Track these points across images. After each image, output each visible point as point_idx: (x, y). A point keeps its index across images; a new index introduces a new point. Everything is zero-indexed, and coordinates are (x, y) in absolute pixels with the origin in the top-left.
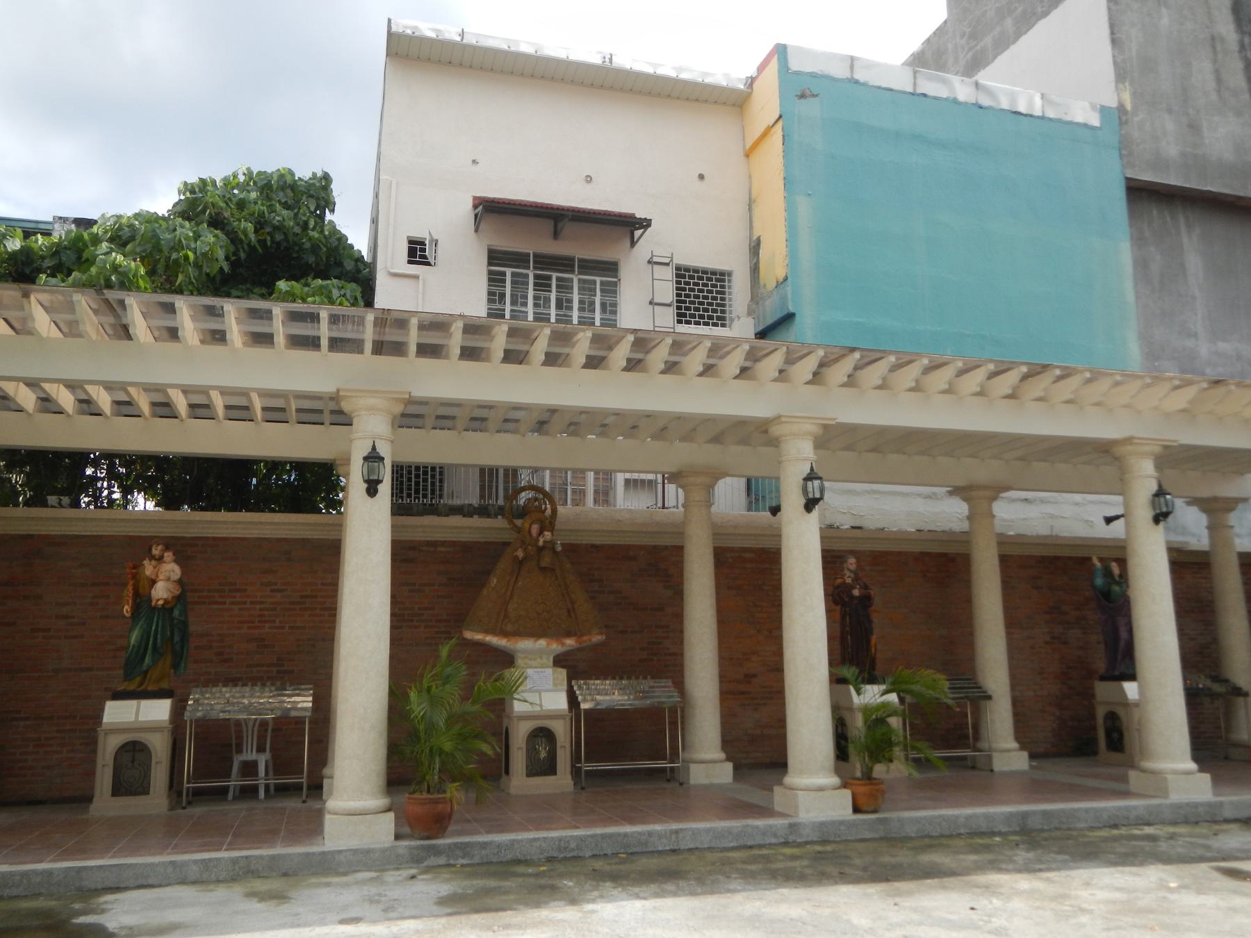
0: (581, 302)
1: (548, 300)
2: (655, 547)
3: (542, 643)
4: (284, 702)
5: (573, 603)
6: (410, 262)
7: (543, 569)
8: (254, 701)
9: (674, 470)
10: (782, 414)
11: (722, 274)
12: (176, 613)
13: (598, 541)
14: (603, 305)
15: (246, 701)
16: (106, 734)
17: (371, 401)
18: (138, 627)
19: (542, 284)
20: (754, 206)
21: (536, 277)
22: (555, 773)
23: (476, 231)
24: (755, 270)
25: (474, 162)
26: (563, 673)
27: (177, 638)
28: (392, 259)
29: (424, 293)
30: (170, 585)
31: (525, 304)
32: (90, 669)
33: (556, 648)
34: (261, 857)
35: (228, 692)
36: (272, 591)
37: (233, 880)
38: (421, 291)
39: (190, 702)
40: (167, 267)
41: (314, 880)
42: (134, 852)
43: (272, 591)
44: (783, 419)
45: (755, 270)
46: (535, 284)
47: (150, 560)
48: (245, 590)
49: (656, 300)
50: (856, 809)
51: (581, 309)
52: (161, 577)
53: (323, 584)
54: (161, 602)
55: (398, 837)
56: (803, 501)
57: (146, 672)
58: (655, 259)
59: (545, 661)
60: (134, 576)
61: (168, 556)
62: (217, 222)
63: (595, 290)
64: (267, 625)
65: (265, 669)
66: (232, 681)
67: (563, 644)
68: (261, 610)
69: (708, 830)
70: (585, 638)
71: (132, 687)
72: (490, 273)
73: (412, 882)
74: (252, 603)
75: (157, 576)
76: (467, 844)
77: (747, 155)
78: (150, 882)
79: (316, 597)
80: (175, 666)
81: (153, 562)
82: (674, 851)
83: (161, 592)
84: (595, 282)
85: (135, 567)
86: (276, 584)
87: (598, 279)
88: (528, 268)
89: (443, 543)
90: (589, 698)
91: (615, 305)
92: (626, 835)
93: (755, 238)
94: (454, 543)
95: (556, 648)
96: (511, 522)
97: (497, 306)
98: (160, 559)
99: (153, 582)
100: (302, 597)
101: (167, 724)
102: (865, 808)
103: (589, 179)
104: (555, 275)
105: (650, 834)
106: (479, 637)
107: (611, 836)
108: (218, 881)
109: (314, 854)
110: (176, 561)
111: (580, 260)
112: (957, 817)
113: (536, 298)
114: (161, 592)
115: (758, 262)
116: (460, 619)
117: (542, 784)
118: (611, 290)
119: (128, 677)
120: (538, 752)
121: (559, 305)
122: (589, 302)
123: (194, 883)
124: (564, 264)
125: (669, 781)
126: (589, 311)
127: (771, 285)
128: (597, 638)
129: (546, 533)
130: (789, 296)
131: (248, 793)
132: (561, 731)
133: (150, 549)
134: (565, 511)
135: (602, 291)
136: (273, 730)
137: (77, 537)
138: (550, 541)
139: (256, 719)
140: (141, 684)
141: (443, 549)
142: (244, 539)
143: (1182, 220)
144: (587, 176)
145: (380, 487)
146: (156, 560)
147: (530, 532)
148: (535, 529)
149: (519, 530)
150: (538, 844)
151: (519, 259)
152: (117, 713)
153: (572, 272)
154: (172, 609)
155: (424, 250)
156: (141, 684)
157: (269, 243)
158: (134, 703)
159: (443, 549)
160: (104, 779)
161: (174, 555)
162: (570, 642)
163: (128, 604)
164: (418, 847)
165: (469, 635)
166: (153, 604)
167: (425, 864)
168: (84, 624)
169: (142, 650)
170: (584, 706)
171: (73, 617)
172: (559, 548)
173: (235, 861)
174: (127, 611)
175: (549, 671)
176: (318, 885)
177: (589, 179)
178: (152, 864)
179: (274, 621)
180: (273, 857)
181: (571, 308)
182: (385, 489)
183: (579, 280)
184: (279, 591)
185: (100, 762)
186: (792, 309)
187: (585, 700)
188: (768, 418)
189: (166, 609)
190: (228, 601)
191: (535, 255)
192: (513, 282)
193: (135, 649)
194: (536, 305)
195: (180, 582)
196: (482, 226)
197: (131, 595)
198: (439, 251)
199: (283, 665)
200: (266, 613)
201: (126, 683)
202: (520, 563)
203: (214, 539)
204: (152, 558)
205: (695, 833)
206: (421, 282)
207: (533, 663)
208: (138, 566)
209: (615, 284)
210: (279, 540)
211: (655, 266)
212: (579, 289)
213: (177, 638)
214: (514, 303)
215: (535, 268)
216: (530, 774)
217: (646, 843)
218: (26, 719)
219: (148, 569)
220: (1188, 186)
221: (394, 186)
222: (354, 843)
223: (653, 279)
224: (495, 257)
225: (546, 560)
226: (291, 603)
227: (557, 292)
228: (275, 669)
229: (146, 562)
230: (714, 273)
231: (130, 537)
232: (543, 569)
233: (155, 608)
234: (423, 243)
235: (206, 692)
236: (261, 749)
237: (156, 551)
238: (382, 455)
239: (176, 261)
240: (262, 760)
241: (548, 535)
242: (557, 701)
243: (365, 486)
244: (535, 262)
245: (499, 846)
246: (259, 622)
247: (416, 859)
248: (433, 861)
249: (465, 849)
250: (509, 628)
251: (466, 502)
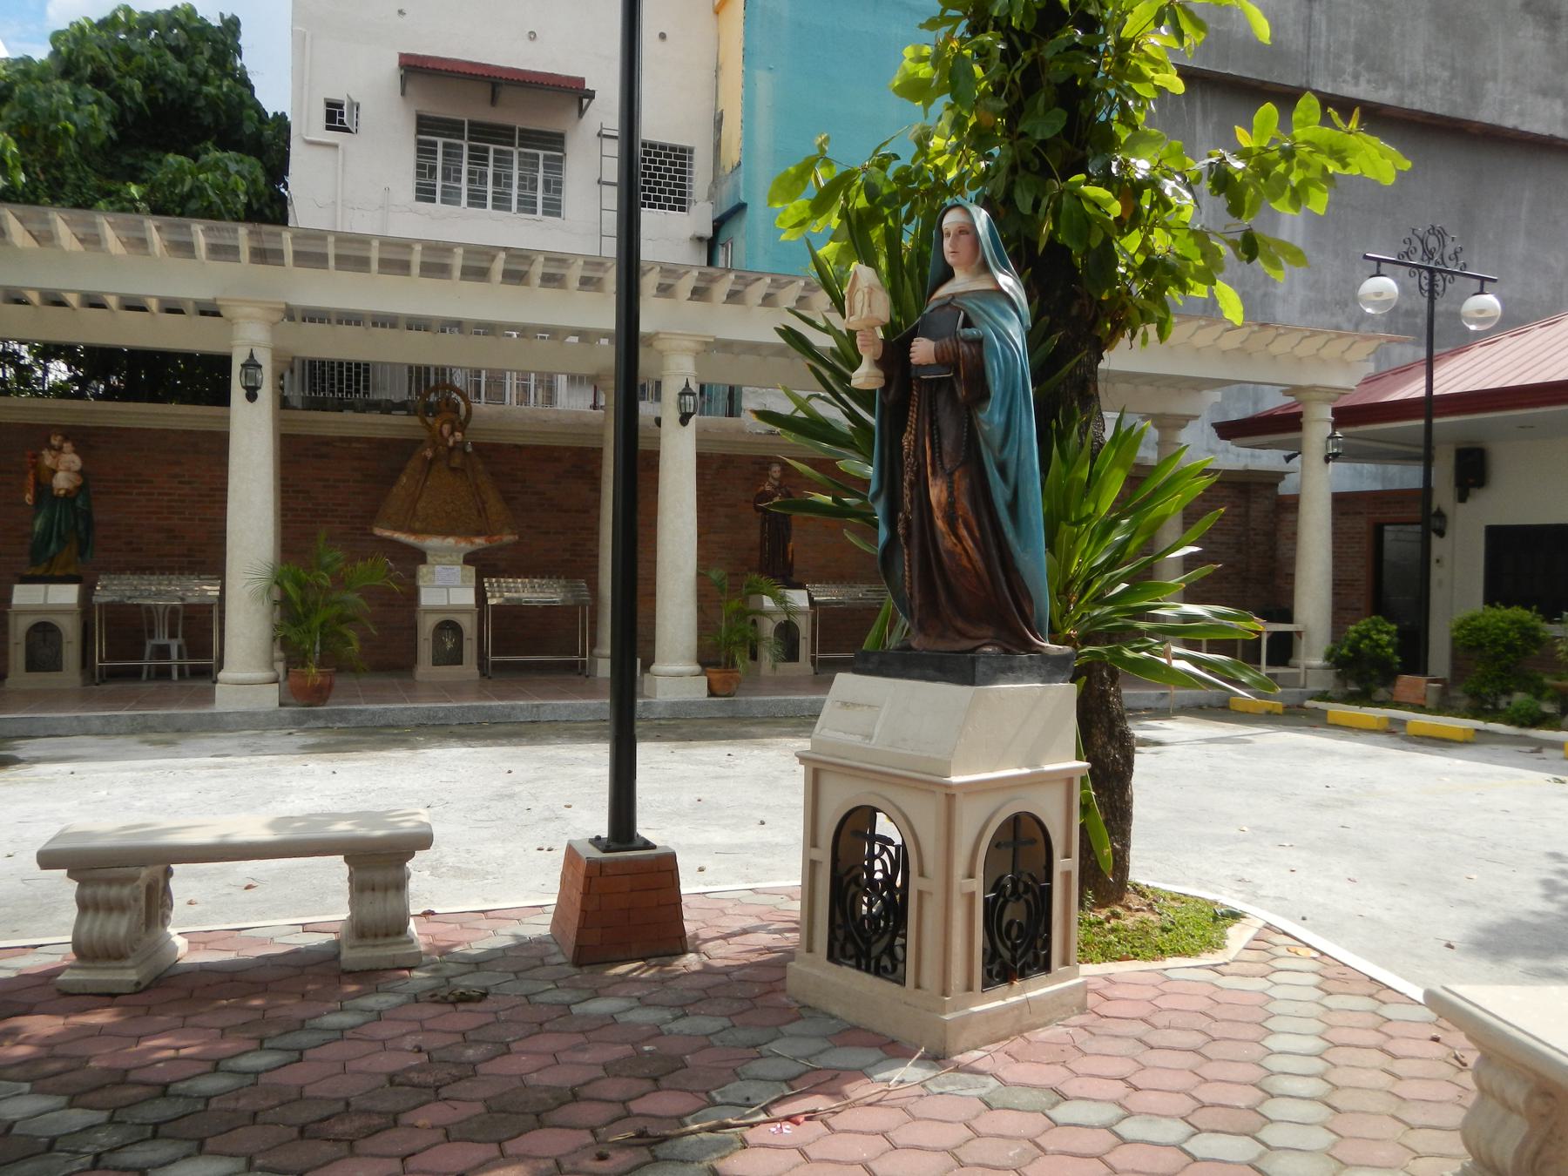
0: (522, 178)
1: (484, 175)
2: (582, 448)
3: (451, 541)
5: (484, 503)
6: (328, 128)
7: (454, 470)
8: (162, 588)
9: (593, 372)
10: (660, 330)
11: (683, 150)
12: (79, 503)
13: (520, 441)
14: (547, 183)
15: (154, 589)
16: (17, 615)
17: (248, 310)
18: (42, 515)
19: (478, 157)
20: (720, 73)
21: (471, 148)
22: (461, 663)
23: (403, 93)
24: (717, 147)
25: (401, 12)
26: (471, 570)
27: (81, 527)
28: (307, 126)
29: (343, 165)
30: (72, 476)
31: (459, 180)
33: (465, 546)
34: (157, 716)
35: (135, 580)
37: (132, 733)
38: (340, 163)
39: (98, 588)
40: (46, 138)
41: (203, 734)
42: (46, 710)
43: (180, 482)
44: (661, 336)
45: (717, 147)
46: (470, 157)
47: (49, 450)
49: (603, 179)
50: (712, 693)
51: (521, 187)
52: (61, 467)
54: (62, 492)
55: (281, 705)
56: (678, 416)
57: (52, 559)
58: (605, 132)
59: (455, 558)
60: (35, 466)
61: (67, 446)
62: (99, 80)
63: (537, 165)
65: (176, 559)
66: (140, 570)
67: (472, 543)
69: (566, 706)
70: (496, 538)
71: (39, 572)
72: (419, 142)
73: (291, 736)
74: (160, 494)
75: (57, 466)
76: (345, 710)
77: (717, 12)
78: (58, 732)
80: (81, 554)
81: (53, 453)
82: (532, 722)
83: (62, 482)
84: (537, 156)
85: (35, 457)
87: (541, 153)
88: (462, 138)
89: (358, 439)
90: (498, 595)
91: (559, 183)
92: (490, 707)
93: (719, 110)
94: (368, 440)
95: (465, 546)
96: (423, 420)
97: (427, 181)
98: (60, 450)
99: (54, 472)
101: (76, 608)
102: (719, 693)
103: (532, 36)
104: (492, 147)
105: (513, 708)
106: (387, 534)
107: (477, 708)
108: (118, 734)
109: (204, 714)
110: (76, 452)
111: (522, 131)
112: (803, 701)
113: (470, 172)
114: (62, 482)
115: (720, 139)
116: (371, 515)
117: (448, 672)
118: (556, 165)
119: (35, 562)
120: (444, 643)
121: (497, 180)
122: (530, 179)
123: (97, 734)
124: (502, 134)
125: (580, 674)
126: (531, 189)
127: (729, 169)
128: (508, 538)
129: (457, 434)
130: (741, 186)
131: (163, 674)
132: (468, 624)
133: (48, 440)
134: (482, 407)
135: (545, 166)
136: (185, 618)
138: (462, 442)
139: (166, 606)
141: (358, 446)
143: (1198, 105)
144: (531, 32)
145: (259, 392)
146: (55, 450)
147: (441, 432)
148: (446, 428)
149: (429, 427)
150: (409, 712)
151: (451, 128)
152: (25, 596)
153: (512, 145)
154: (74, 500)
155: (342, 114)
157: (161, 101)
158: (41, 587)
159: (358, 446)
160: (17, 656)
161: (74, 445)
162: (480, 542)
164: (299, 712)
165: (378, 531)
166: (55, 493)
167: (306, 726)
170: (491, 602)
172: (469, 449)
173: (133, 718)
175: (458, 568)
176: (204, 737)
177: (532, 36)
178: (60, 718)
180: (168, 715)
181: (510, 186)
182: (266, 393)
183: (520, 153)
184: (189, 483)
185: (12, 641)
186: (743, 199)
187: (493, 597)
188: (650, 334)
189: (69, 498)
190: (135, 491)
191: (471, 124)
192: (445, 154)
194: (471, 181)
195: (81, 472)
196: (409, 88)
198: (360, 115)
200: (174, 504)
202: (431, 462)
203: (118, 429)
204: (51, 448)
205: (553, 707)
206: (340, 151)
207: (443, 560)
208: (37, 456)
209: (560, 159)
210: (185, 432)
211: (604, 140)
212: (520, 164)
213: (81, 527)
214: (446, 177)
215: (470, 139)
216: (436, 663)
217: (509, 716)
219: (48, 459)
220: (1205, 68)
221: (308, 39)
222: (242, 708)
223: (602, 156)
224: (425, 124)
225: (456, 461)
227: (495, 166)
229: (45, 453)
230: (673, 149)
232: (454, 470)
233: (57, 497)
234: (340, 106)
235: (115, 579)
236: (173, 635)
237: (55, 441)
238: (260, 362)
239: (55, 133)
240: (174, 646)
241: (458, 435)
242: (467, 597)
243: (244, 392)
244: (470, 131)
245: (373, 713)
247: (298, 723)
248: (312, 724)
249: (342, 715)
250: (417, 525)
251: (384, 398)
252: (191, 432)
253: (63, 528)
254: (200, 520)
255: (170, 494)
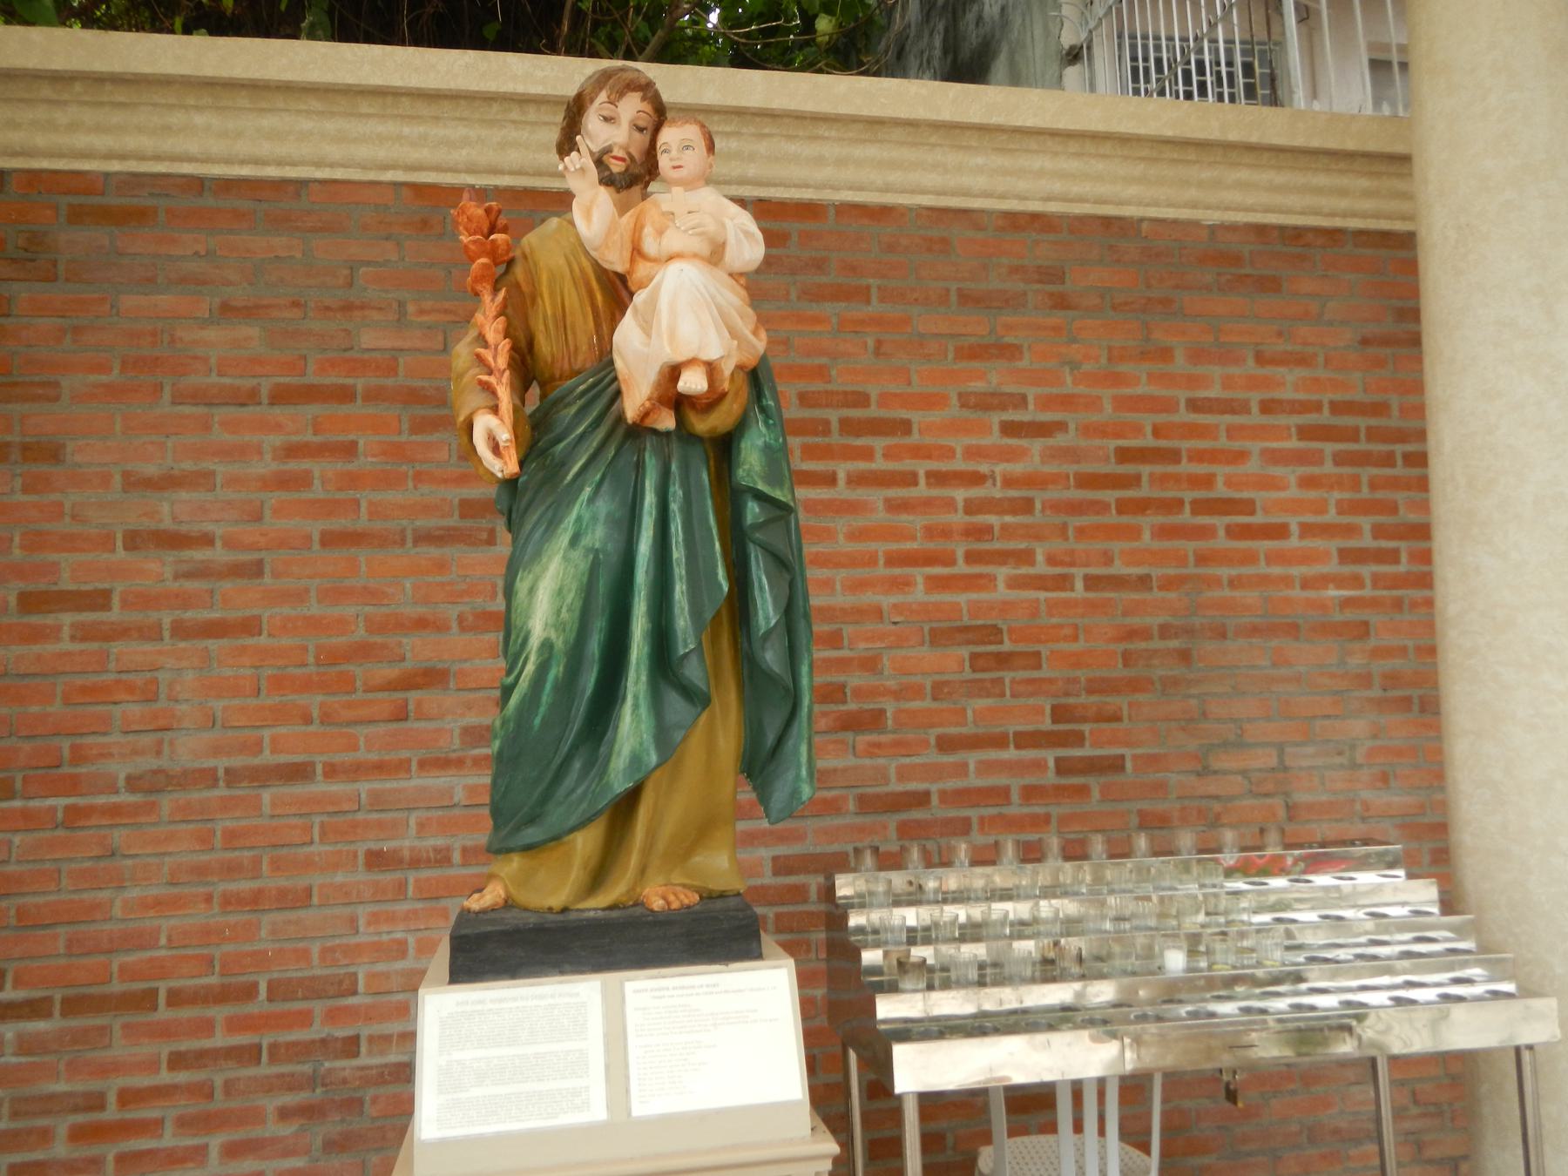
4: (594, 791)
18: (563, 538)
32: (299, 772)
36: (1009, 429)
43: (1009, 429)
48: (905, 427)
53: (1194, 405)
57: (631, 799)
64: (1002, 572)
65: (1011, 754)
68: (971, 507)
74: (937, 478)
79: (1173, 456)
86: (1021, 401)
100: (1124, 455)
137: (198, 184)
140: (598, 877)
142: (882, 213)
156: (598, 877)
163: (495, 410)
168: (256, 569)
169: (589, 680)
171: (207, 540)
174: (496, 449)
179: (1026, 557)
190: (842, 469)
193: (556, 671)
197: (502, 362)
199: (1078, 739)
200: (993, 519)
201: (514, 865)
210: (1015, 221)
218: (35, 1009)
226: (1086, 481)
228: (1050, 756)
231: (418, 189)
246: (971, 557)
252: (1036, 220)
253: (682, 621)
254: (1092, 582)
255: (977, 479)
